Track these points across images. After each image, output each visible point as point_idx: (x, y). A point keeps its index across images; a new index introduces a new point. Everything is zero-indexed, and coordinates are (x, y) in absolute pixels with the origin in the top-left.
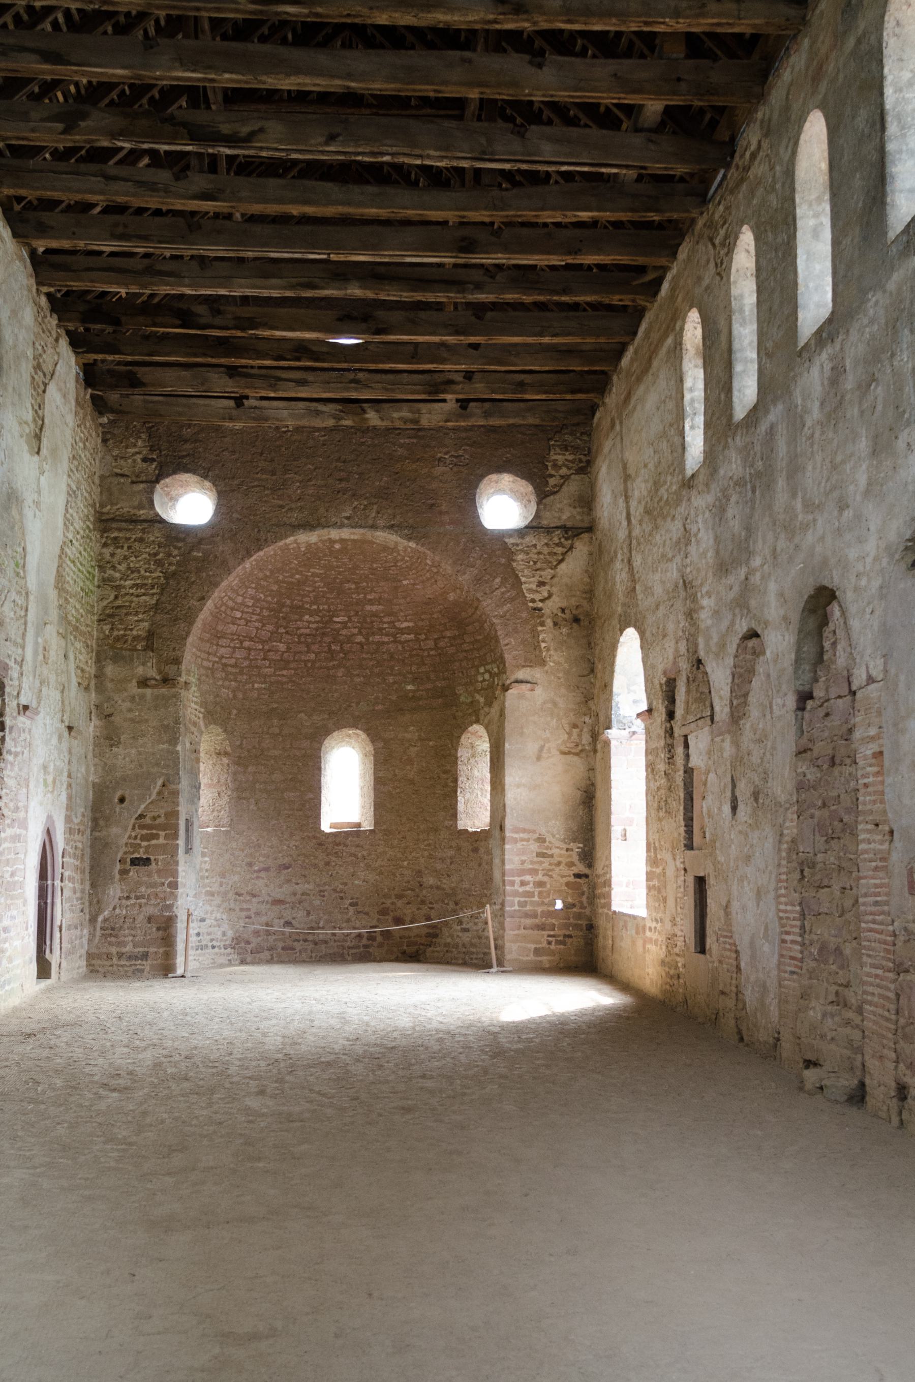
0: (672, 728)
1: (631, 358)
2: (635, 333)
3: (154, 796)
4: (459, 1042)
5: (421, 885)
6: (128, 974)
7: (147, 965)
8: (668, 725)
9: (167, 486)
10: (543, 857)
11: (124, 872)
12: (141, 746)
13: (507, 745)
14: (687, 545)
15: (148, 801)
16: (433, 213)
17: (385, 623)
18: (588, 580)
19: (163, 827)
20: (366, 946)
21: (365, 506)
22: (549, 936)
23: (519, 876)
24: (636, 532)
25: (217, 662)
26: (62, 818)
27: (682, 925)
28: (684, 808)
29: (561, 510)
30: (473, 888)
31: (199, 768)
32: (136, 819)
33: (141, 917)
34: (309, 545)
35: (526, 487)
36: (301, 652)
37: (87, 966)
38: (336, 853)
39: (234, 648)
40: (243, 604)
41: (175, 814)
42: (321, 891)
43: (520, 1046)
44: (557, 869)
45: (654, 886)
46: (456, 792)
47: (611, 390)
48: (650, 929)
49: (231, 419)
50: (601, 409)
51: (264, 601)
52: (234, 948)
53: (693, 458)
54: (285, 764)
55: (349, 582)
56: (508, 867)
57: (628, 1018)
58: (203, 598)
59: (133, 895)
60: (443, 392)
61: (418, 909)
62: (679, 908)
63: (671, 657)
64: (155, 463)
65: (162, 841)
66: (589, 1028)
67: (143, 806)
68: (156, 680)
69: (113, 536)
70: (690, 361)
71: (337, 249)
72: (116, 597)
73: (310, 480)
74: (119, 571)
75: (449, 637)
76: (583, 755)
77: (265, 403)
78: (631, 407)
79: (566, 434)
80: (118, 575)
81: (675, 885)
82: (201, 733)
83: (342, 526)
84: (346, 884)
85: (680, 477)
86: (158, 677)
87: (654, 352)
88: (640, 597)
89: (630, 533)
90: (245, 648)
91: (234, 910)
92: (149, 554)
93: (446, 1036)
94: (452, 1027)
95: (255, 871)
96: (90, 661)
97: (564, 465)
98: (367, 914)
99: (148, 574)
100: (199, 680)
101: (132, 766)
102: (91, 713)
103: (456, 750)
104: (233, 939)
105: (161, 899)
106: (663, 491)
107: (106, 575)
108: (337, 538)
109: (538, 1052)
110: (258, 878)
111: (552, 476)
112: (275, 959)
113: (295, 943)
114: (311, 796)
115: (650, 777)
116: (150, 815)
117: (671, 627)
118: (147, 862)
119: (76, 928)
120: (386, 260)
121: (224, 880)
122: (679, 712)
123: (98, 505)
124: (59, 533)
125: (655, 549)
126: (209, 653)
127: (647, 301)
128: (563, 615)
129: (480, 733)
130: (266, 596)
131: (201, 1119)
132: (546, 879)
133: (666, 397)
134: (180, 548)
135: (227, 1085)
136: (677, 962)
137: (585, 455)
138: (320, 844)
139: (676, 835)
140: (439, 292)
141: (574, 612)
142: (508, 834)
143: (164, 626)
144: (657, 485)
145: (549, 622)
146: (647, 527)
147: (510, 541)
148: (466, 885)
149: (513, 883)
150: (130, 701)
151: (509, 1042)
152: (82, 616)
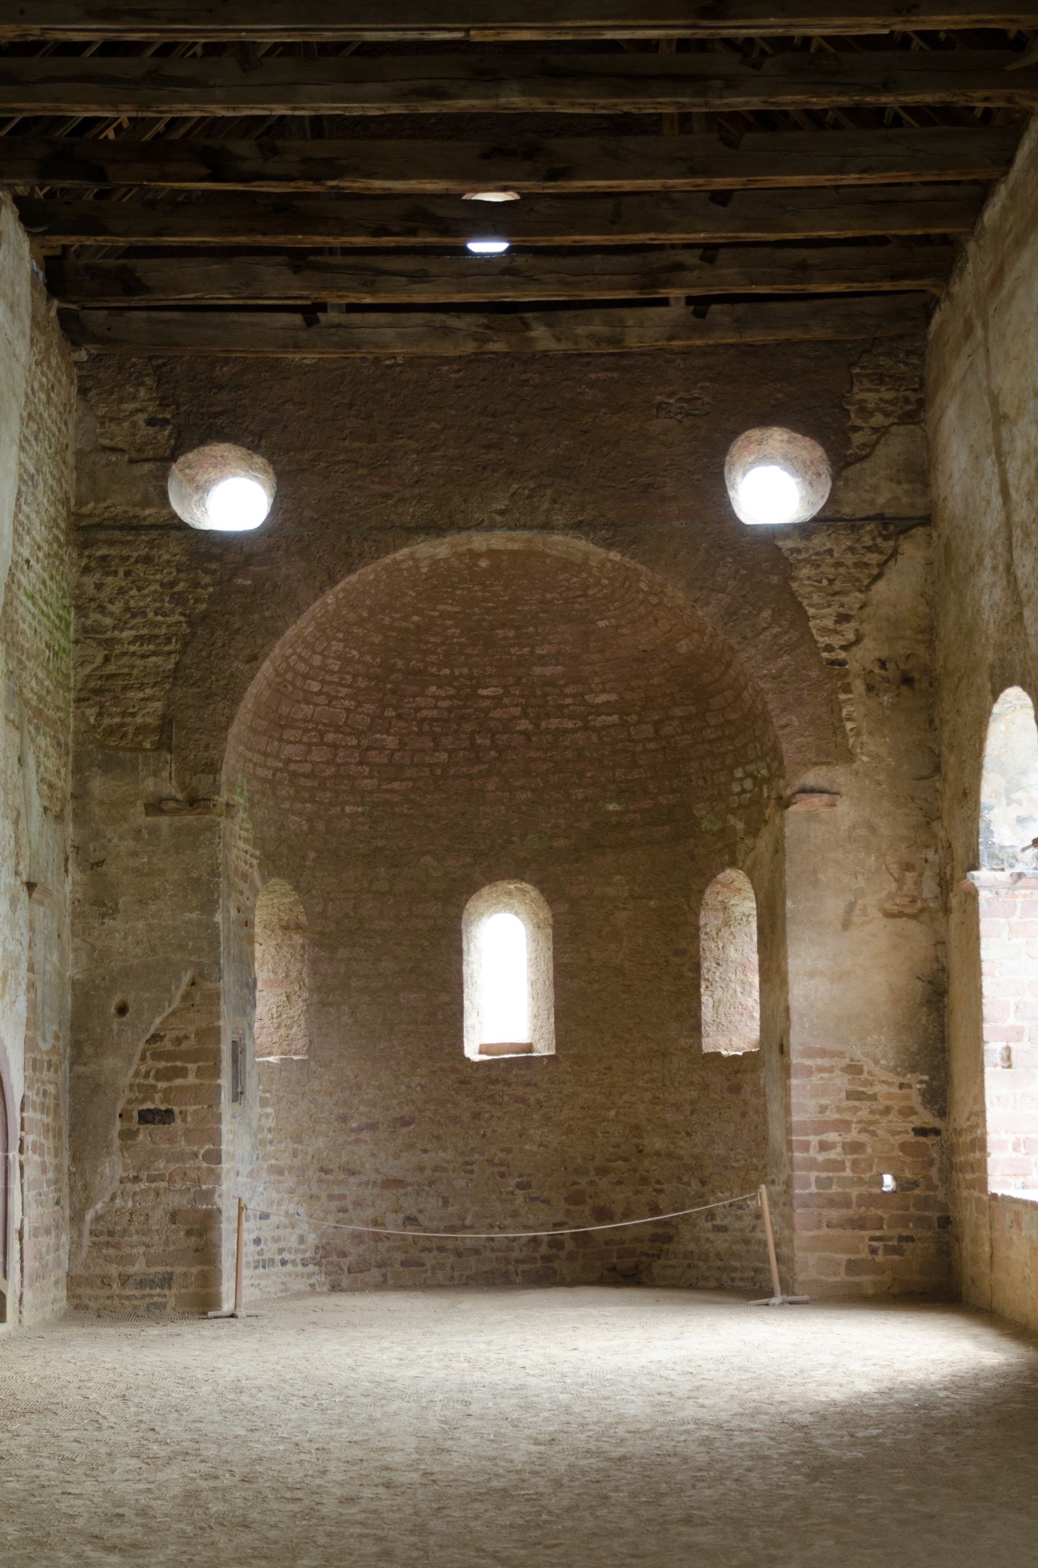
2: (1010, 162)
3: (176, 1003)
4: (742, 1445)
5: (640, 1151)
6: (139, 1313)
9: (190, 467)
10: (859, 1099)
11: (127, 1135)
12: (153, 916)
13: (789, 903)
15: (170, 1010)
17: (567, 696)
18: (927, 610)
19: (193, 1056)
20: (546, 1258)
21: (532, 490)
25: (281, 770)
29: (875, 488)
30: (732, 1154)
31: (253, 953)
32: (147, 1042)
33: (158, 1214)
34: (435, 562)
35: (811, 450)
36: (421, 750)
37: (68, 1298)
38: (492, 1097)
39: (310, 744)
40: (323, 667)
41: (215, 1033)
42: (467, 1163)
43: (858, 1453)
44: (884, 1121)
46: (698, 987)
47: (962, 270)
49: (297, 346)
50: (945, 305)
52: (318, 1264)
54: (399, 944)
55: (503, 625)
56: (796, 1118)
58: (254, 658)
59: (144, 1175)
60: (667, 284)
61: (637, 1192)
64: (170, 427)
65: (191, 1079)
66: (978, 1414)
67: (158, 1021)
68: (177, 801)
69: (99, 553)
71: (483, 21)
72: (107, 659)
73: (435, 448)
74: (112, 614)
75: (680, 718)
76: (925, 917)
77: (355, 318)
78: (1004, 292)
80: (108, 621)
82: (256, 892)
83: (492, 527)
84: (509, 1151)
86: (180, 796)
89: (1008, 517)
90: (327, 745)
91: (318, 1198)
92: (162, 585)
93: (716, 1435)
94: (724, 1416)
95: (352, 1130)
96: (63, 771)
97: (878, 409)
98: (547, 1202)
99: (159, 618)
100: (250, 800)
102: (67, 859)
103: (697, 915)
104: (317, 1248)
105: (193, 1180)
107: (89, 622)
108: (484, 548)
110: (357, 1141)
111: (856, 429)
112: (390, 1282)
113: (423, 1255)
114: (446, 998)
116: (170, 1035)
118: (166, 1116)
119: (48, 1232)
120: (569, 37)
121: (299, 1147)
123: (73, 502)
126: (266, 754)
128: (883, 672)
129: (737, 885)
132: (864, 1138)
134: (213, 572)
135: (322, 1540)
137: (914, 390)
138: (463, 1082)
140: (662, 95)
141: (902, 666)
142: (795, 1059)
143: (189, 707)
145: (859, 686)
147: (786, 545)
148: (720, 1150)
150: (134, 839)
151: (833, 1445)
152: (48, 692)
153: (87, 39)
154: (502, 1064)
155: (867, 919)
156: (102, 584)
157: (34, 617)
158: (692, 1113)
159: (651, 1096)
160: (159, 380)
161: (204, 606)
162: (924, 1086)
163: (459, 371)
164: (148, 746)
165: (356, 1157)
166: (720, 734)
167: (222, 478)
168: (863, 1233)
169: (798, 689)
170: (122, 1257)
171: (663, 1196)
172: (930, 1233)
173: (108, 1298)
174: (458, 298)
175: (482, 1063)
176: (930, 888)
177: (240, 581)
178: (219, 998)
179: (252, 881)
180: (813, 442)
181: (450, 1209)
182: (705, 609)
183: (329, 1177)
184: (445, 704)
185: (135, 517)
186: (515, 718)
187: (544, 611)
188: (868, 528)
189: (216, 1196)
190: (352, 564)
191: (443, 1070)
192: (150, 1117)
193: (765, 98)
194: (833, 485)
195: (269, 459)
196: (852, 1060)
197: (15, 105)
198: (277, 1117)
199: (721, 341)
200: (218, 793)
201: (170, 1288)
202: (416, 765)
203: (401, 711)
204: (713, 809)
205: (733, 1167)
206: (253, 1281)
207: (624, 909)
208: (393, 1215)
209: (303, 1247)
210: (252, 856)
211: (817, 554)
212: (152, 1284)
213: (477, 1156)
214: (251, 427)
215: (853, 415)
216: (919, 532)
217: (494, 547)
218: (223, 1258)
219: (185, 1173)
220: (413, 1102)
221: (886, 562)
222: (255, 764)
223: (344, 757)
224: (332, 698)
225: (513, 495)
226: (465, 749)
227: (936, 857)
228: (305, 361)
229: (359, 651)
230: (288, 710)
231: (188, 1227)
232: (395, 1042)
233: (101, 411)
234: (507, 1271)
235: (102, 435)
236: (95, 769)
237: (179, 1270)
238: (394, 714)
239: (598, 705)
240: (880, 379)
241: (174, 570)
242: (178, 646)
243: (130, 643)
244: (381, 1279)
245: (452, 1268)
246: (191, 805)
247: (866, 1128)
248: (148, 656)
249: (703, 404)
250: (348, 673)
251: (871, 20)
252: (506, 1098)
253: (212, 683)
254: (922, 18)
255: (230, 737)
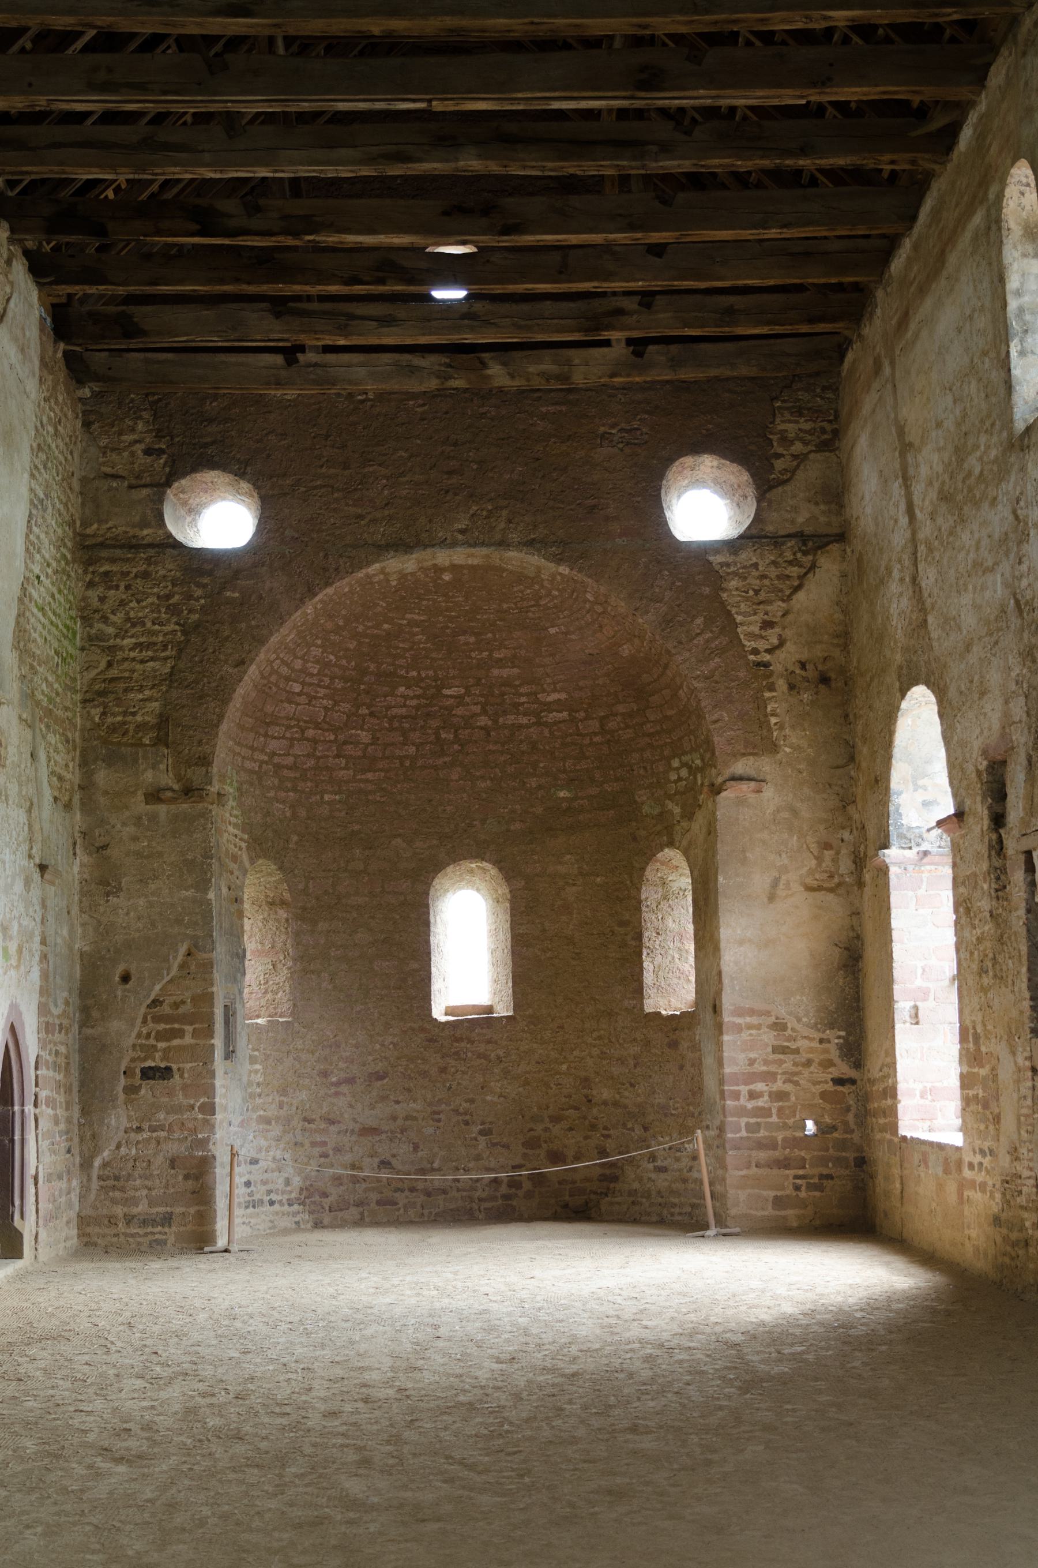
0: (1000, 841)
1: (908, 258)
2: (914, 218)
3: (174, 971)
4: (681, 1362)
5: (590, 1101)
6: (143, 1249)
7: (171, 1233)
8: (994, 837)
9: (183, 492)
10: (784, 1053)
11: (131, 1090)
12: (153, 894)
13: (721, 879)
14: (1020, 543)
15: (167, 979)
16: (598, 21)
17: (522, 695)
18: (842, 617)
20: (506, 1197)
21: (490, 511)
22: (796, 1177)
23: (746, 1084)
24: (926, 531)
25: (266, 763)
26: (34, 1007)
27: (1031, 1160)
28: (1029, 970)
31: (242, 926)
33: (159, 1160)
34: (403, 576)
36: (392, 744)
37: (79, 1236)
38: (457, 1053)
39: (292, 739)
40: (304, 671)
41: (208, 998)
42: (435, 1113)
44: (806, 1073)
45: (976, 1096)
46: (640, 954)
47: (872, 314)
48: (971, 1166)
49: (279, 384)
51: (335, 665)
52: (303, 1204)
53: (1026, 403)
54: (373, 918)
55: (464, 633)
56: (727, 1070)
57: (948, 1313)
59: (146, 1126)
60: (608, 328)
61: (586, 1138)
62: (1023, 1133)
63: (996, 726)
64: (165, 456)
65: (188, 1040)
66: (891, 1332)
67: (158, 987)
68: (173, 791)
69: (102, 570)
70: (1015, 247)
71: (444, 93)
72: (110, 664)
73: (402, 474)
74: (114, 624)
75: (623, 714)
76: (842, 891)
77: (331, 358)
78: (909, 334)
79: (799, 390)
80: (111, 630)
81: (1015, 1096)
82: (245, 872)
83: (454, 544)
84: (472, 1101)
85: (1005, 434)
86: (176, 787)
87: (949, 241)
88: (934, 635)
89: (914, 533)
90: (308, 740)
91: (302, 1145)
92: (159, 597)
93: (658, 1352)
94: (665, 1336)
95: (333, 1084)
96: (71, 765)
98: (506, 1146)
99: (157, 627)
100: (239, 789)
101: (140, 925)
102: (75, 844)
103: (639, 890)
104: (301, 1189)
105: (190, 1130)
106: (973, 463)
107: (94, 631)
108: (447, 563)
109: (816, 1379)
110: (337, 1094)
111: (778, 456)
112: (367, 1220)
113: (397, 1195)
115: (963, 920)
116: (169, 1000)
117: (994, 678)
118: (166, 1073)
119: (60, 1177)
120: (521, 107)
121: (285, 1099)
122: (1015, 811)
123: (78, 523)
124: (18, 563)
125: (963, 554)
126: (253, 749)
127: (936, 162)
128: (803, 673)
130: (338, 658)
131: (268, 1516)
132: (789, 1087)
133: (974, 310)
134: (205, 586)
135: (308, 1450)
136: (1023, 1220)
137: (830, 421)
138: (430, 1040)
139: (1014, 1013)
140: (604, 159)
141: (820, 667)
142: (727, 1018)
143: (183, 707)
144: (960, 452)
145: (781, 684)
146: (945, 522)
147: (717, 559)
148: (660, 1099)
149: (736, 1096)
150: (135, 825)
151: (763, 1361)
152: (58, 694)
153: (89, 109)
154: (466, 1024)
155: (790, 893)
156: (105, 597)
157: (44, 626)
158: (635, 1067)
159: (598, 1052)
160: (155, 415)
161: (197, 616)
162: (841, 1041)
163: (424, 405)
164: (148, 742)
165: (335, 1108)
166: (658, 728)
167: (212, 501)
168: (787, 1172)
169: (728, 688)
170: (127, 1199)
171: (610, 1140)
172: (847, 1172)
173: (115, 1235)
174: (423, 340)
175: (448, 1023)
176: (845, 865)
177: (228, 594)
178: (212, 968)
179: (242, 862)
180: (740, 468)
181: (420, 1154)
182: (645, 617)
183: (312, 1126)
184: (414, 702)
185: (134, 537)
186: (474, 715)
187: (500, 620)
188: (789, 544)
189: (211, 1144)
190: (329, 578)
191: (413, 1030)
192: (151, 1073)
193: (695, 162)
194: (758, 506)
195: (254, 485)
196: (777, 1018)
197: (25, 169)
198: (264, 1073)
199: (657, 378)
200: (211, 783)
201: (170, 1226)
202: (388, 758)
203: (373, 709)
204: (653, 794)
205: (672, 1115)
206: (244, 1219)
207: (574, 885)
208: (369, 1160)
209: (289, 1188)
210: (241, 839)
211: (744, 567)
212: (154, 1223)
213: (443, 1106)
214: (238, 456)
215: (775, 444)
216: (834, 547)
217: (456, 562)
218: (218, 1199)
219: (183, 1124)
220: (385, 1058)
221: (806, 574)
222: (244, 758)
223: (322, 751)
224: (311, 698)
225: (473, 515)
226: (431, 743)
227: (851, 837)
228: (288, 397)
229: (336, 656)
230: (272, 709)
231: (185, 1172)
232: (370, 1005)
233: (103, 442)
234: (471, 1209)
235: (104, 464)
236: (99, 763)
237: (178, 1210)
238: (367, 711)
239: (550, 703)
240: (799, 412)
241: (169, 584)
242: (174, 653)
243: (130, 650)
244: (359, 1217)
245: (422, 1207)
246: (186, 794)
247: (790, 1078)
248: (147, 661)
249: (642, 434)
250: (326, 675)
251: (789, 92)
252: (469, 1054)
253: (204, 685)
254: (835, 89)
255: (220, 734)
